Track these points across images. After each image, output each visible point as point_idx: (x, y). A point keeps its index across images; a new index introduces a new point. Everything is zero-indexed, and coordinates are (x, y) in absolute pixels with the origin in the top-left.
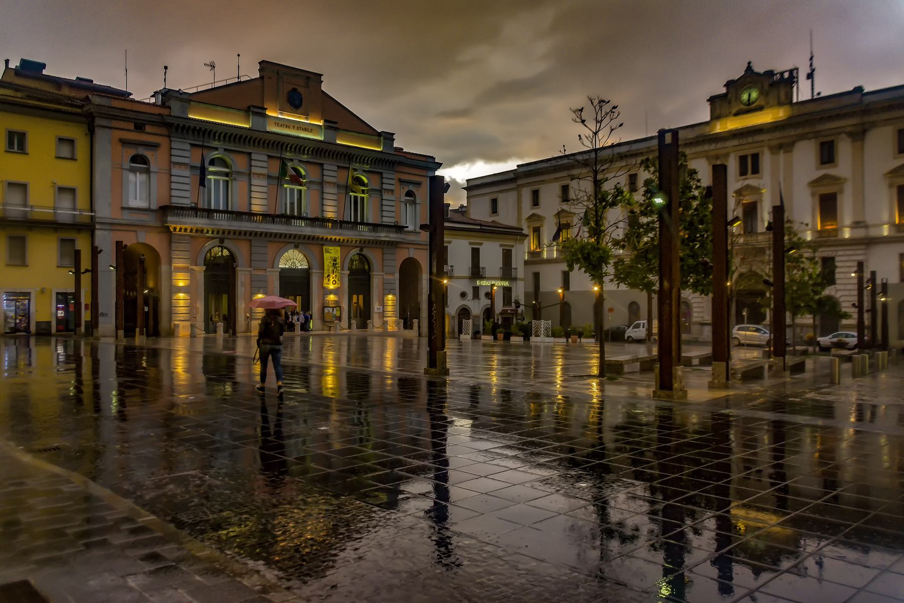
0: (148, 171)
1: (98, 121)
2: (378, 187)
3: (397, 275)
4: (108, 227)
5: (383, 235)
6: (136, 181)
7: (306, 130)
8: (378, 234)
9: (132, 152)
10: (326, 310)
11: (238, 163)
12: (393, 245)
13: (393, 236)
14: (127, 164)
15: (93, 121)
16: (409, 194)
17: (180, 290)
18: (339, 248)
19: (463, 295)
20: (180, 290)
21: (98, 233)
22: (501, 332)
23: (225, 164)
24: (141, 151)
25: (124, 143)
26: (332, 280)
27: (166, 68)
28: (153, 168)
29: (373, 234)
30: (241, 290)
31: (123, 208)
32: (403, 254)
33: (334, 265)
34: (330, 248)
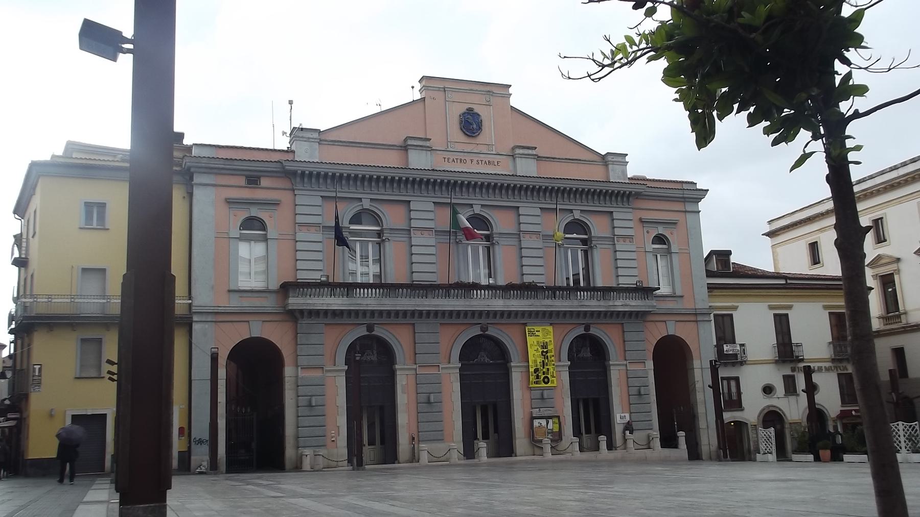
0: (265, 239)
1: (197, 179)
3: (650, 364)
5: (618, 303)
6: (249, 253)
8: (611, 303)
9: (243, 215)
10: (536, 423)
11: (392, 217)
13: (635, 304)
14: (235, 232)
15: (191, 179)
16: (660, 239)
18: (550, 329)
19: (768, 390)
21: (196, 327)
22: (825, 448)
23: (377, 220)
24: (255, 212)
27: (291, 102)
28: (272, 233)
29: (602, 303)
31: (229, 291)
32: (656, 332)
33: (544, 354)
34: (536, 328)
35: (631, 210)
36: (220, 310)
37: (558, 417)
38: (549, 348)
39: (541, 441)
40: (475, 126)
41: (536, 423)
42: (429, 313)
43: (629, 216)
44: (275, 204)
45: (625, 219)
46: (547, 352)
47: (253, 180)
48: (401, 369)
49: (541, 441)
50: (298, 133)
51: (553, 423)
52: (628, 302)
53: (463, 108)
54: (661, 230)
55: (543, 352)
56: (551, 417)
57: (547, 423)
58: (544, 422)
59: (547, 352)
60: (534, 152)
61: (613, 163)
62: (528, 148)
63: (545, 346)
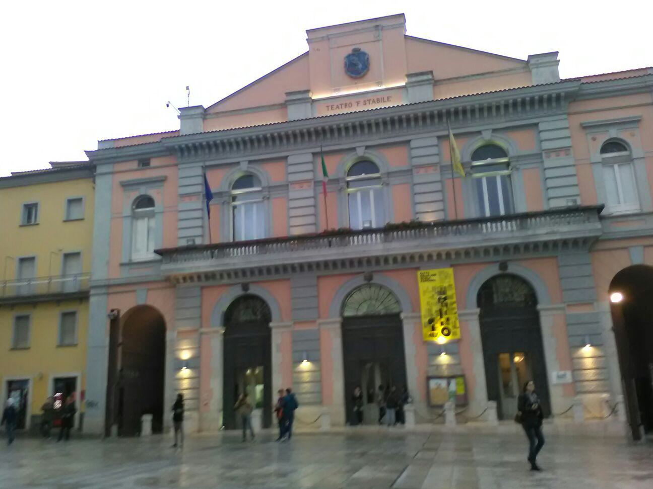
2: (535, 151)
4: (104, 291)
7: (378, 101)
8: (530, 232)
9: (134, 194)
12: (587, 245)
17: (188, 364)
18: (450, 271)
20: (188, 364)
24: (143, 191)
25: (125, 185)
26: (439, 328)
27: (187, 88)
30: (277, 358)
33: (443, 301)
34: (432, 272)
35: (565, 116)
36: (112, 282)
37: (463, 376)
38: (449, 293)
39: (441, 406)
40: (360, 66)
41: (433, 384)
42: (301, 266)
43: (565, 124)
44: (162, 180)
45: (555, 128)
46: (445, 299)
47: (145, 163)
48: (279, 327)
49: (441, 406)
50: (186, 113)
51: (457, 384)
52: (556, 228)
53: (349, 50)
54: (613, 133)
55: (439, 299)
56: (453, 377)
57: (449, 384)
58: (443, 383)
59: (445, 299)
60: (430, 77)
61: (537, 66)
62: (422, 74)
63: (442, 291)
